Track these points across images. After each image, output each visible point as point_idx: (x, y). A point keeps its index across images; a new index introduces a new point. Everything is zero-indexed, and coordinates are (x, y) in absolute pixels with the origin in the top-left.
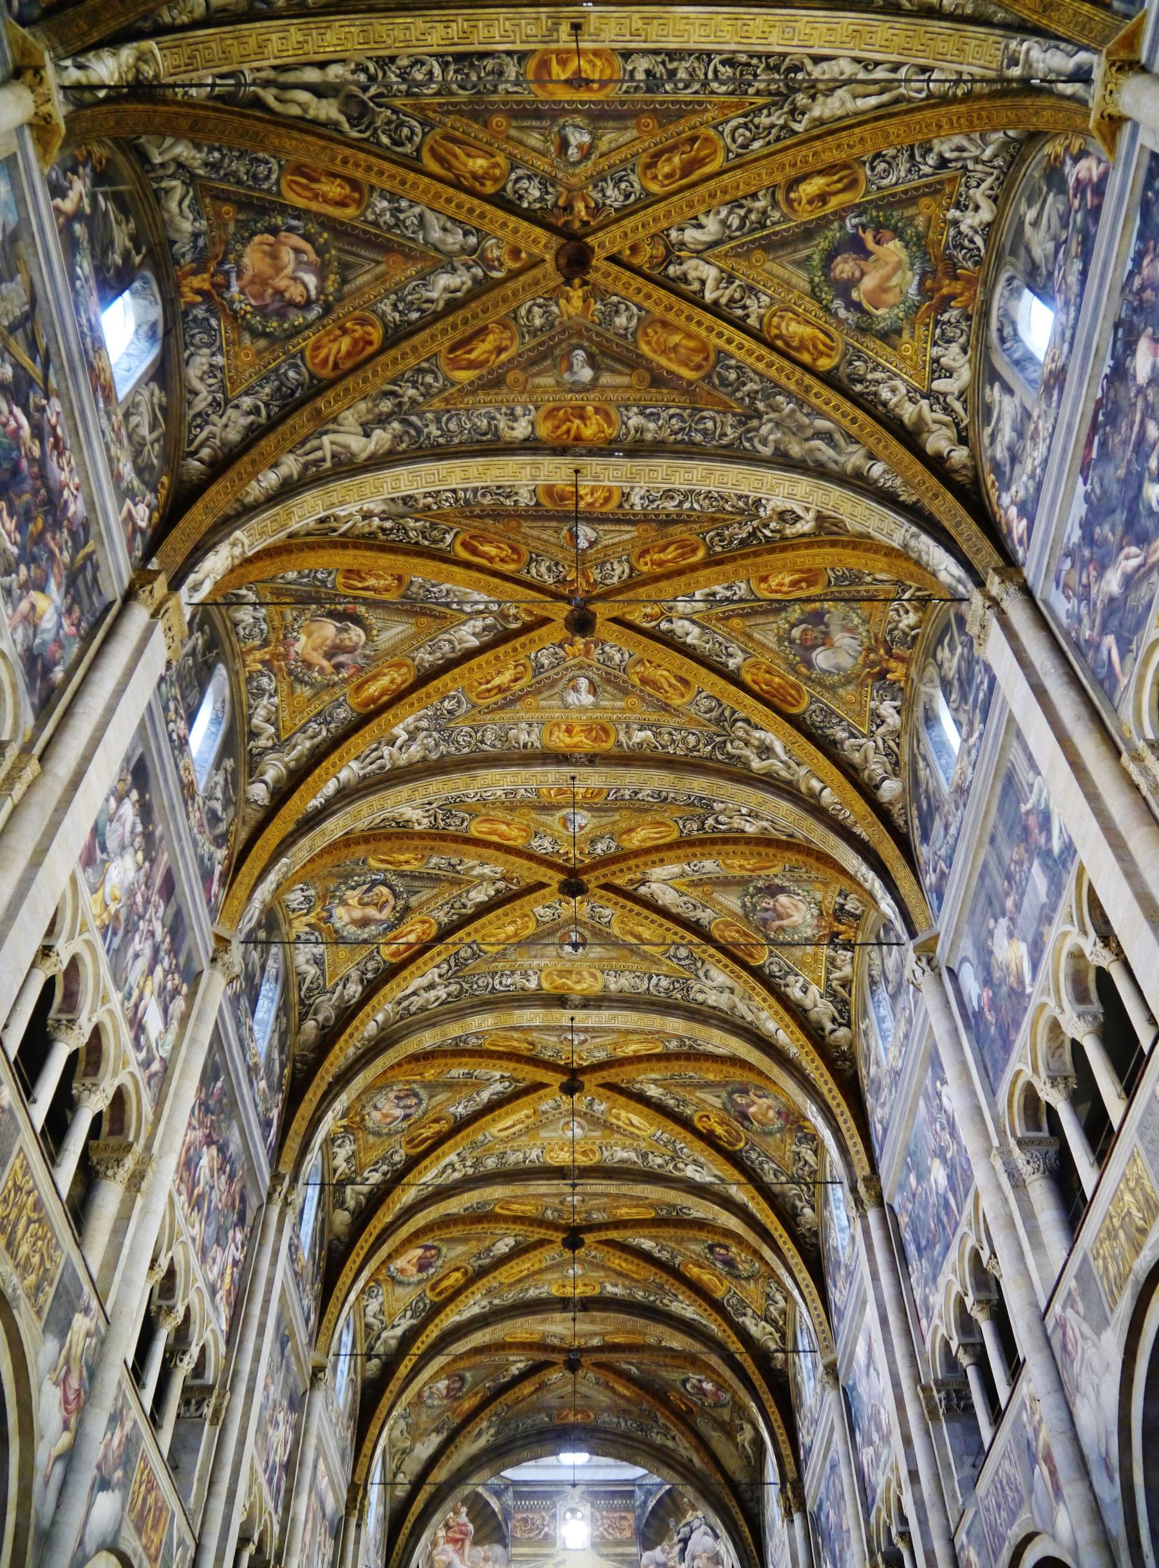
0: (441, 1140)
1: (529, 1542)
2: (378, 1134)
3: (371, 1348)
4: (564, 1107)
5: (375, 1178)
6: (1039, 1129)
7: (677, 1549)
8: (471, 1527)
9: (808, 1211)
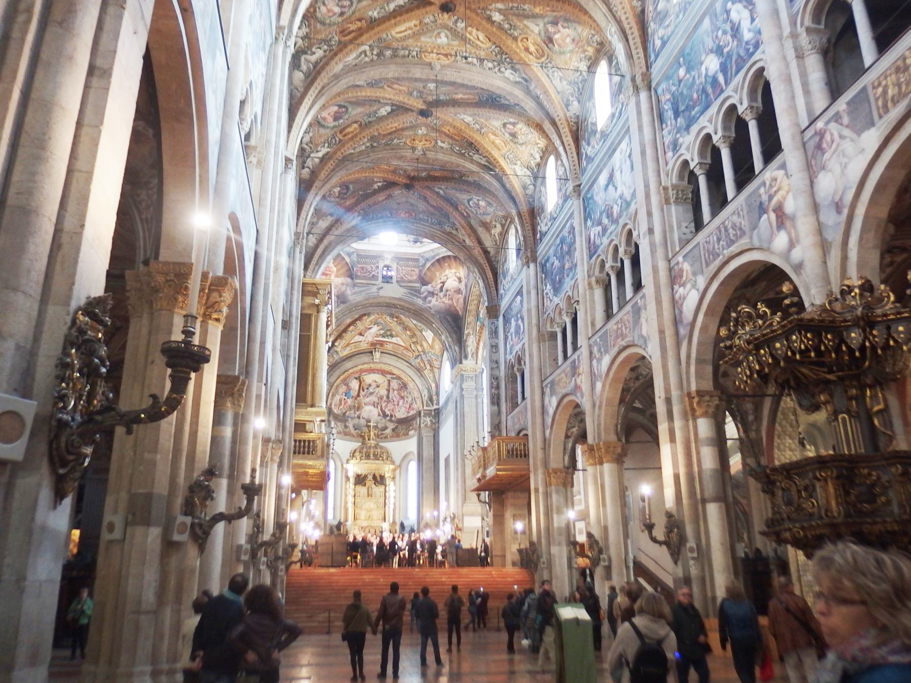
0: (360, 32)
1: (365, 278)
2: (323, 23)
3: (304, 162)
4: (439, 22)
5: (319, 53)
6: (819, 23)
7: (439, 286)
8: (335, 269)
9: (576, 103)
